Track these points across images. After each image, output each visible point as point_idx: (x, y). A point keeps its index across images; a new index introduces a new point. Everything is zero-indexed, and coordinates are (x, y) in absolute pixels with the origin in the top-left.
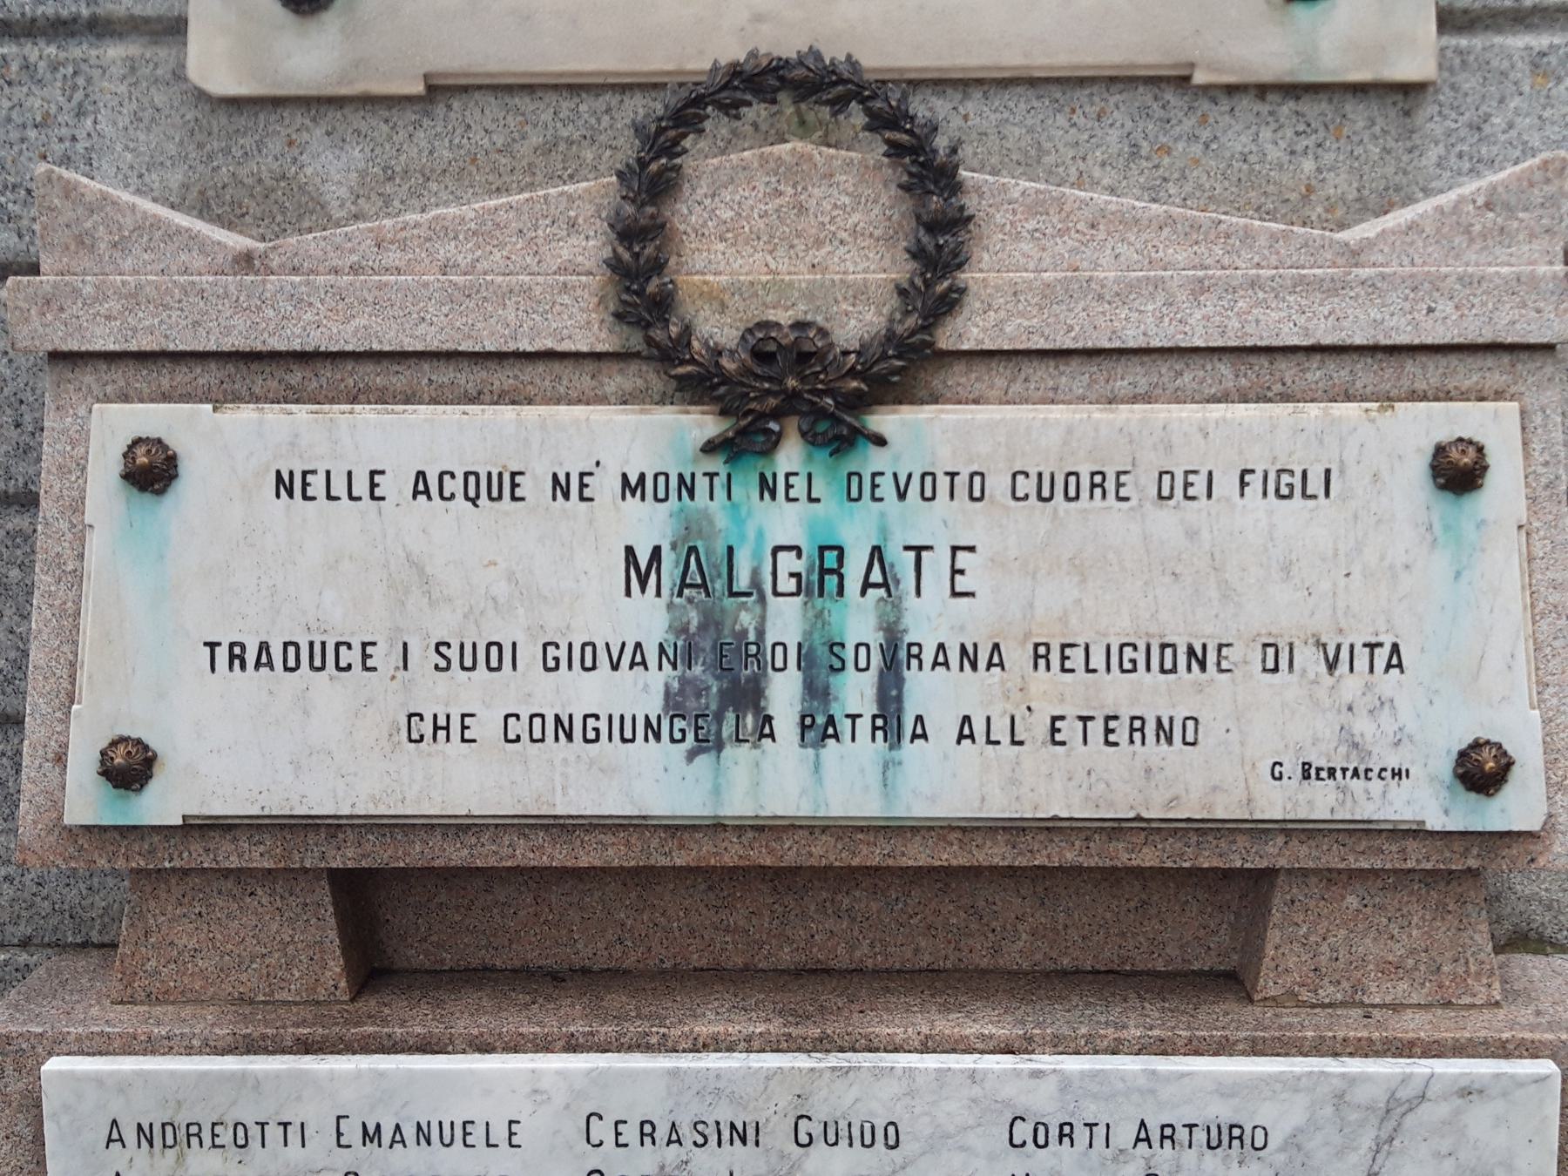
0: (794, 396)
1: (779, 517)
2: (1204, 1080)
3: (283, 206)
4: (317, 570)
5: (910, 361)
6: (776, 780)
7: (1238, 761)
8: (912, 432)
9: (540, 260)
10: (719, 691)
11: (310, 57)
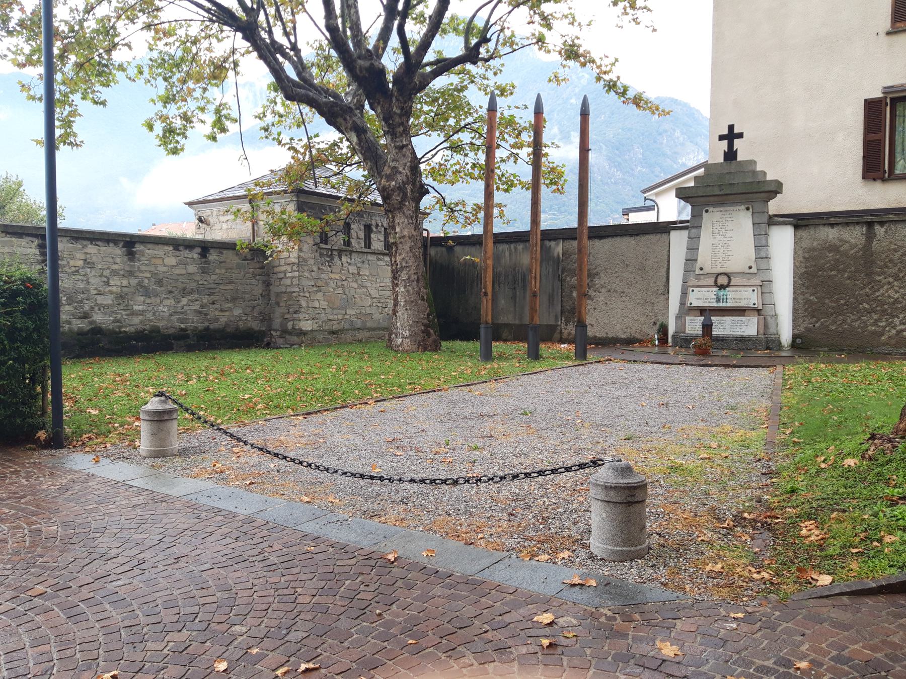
0: (722, 287)
1: (721, 293)
2: (740, 318)
3: (700, 279)
4: (700, 295)
5: (728, 286)
6: (721, 304)
7: (743, 304)
8: (728, 289)
9: (711, 281)
10: (718, 300)
11: (701, 272)
